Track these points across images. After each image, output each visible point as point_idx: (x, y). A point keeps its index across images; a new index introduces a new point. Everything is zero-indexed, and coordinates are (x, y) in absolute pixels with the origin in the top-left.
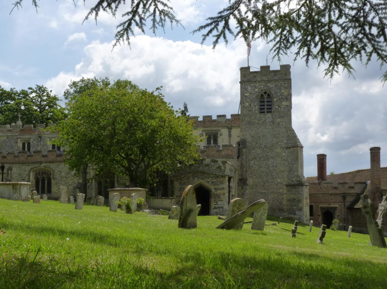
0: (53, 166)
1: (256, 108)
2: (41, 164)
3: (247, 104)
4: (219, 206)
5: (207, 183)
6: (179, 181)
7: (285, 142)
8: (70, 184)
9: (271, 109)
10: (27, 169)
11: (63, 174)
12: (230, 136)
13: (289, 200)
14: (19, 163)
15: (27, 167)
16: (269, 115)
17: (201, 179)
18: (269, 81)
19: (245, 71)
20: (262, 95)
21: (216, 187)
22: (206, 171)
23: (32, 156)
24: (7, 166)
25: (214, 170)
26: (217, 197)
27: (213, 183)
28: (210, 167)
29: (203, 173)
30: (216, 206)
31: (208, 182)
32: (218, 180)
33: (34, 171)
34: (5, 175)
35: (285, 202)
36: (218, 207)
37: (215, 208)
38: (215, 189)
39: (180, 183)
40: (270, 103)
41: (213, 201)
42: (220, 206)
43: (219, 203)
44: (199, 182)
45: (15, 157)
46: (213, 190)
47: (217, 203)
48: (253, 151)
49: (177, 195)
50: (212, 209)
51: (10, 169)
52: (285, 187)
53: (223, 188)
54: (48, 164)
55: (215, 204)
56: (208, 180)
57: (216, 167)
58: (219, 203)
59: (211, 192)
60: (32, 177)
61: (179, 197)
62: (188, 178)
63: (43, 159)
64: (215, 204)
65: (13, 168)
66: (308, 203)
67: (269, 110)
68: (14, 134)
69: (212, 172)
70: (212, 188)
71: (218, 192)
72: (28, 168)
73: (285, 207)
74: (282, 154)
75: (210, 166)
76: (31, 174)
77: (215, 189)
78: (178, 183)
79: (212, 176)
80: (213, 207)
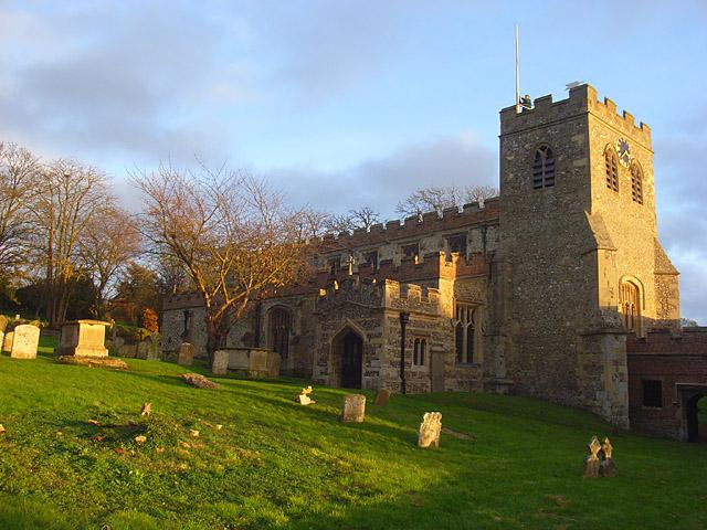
1: (527, 182)
3: (511, 176)
7: (578, 242)
9: (553, 178)
12: (485, 241)
13: (586, 367)
16: (549, 191)
18: (549, 124)
19: (507, 114)
20: (538, 155)
21: (370, 332)
29: (354, 306)
31: (359, 323)
35: (580, 372)
37: (368, 374)
39: (325, 328)
40: (552, 168)
43: (373, 363)
46: (365, 339)
47: (369, 362)
48: (521, 266)
51: (192, 315)
52: (579, 339)
53: (379, 335)
58: (373, 363)
66: (622, 374)
67: (551, 182)
73: (579, 383)
74: (573, 268)
80: (364, 371)
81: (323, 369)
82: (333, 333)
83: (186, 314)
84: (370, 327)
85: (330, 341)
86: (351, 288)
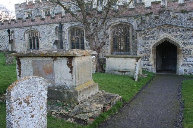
0: (39, 28)
2: (31, 27)
4: (188, 63)
5: (173, 37)
6: (143, 36)
8: (51, 41)
10: (23, 31)
11: (46, 34)
14: (18, 27)
15: (23, 29)
17: (167, 33)
21: (185, 41)
22: (174, 24)
23: (25, 21)
24: (11, 30)
25: (184, 23)
26: (187, 53)
27: (181, 37)
28: (178, 20)
29: (170, 26)
30: (186, 63)
31: (176, 36)
32: (189, 34)
33: (27, 33)
34: (10, 37)
36: (187, 64)
37: (184, 65)
38: (184, 43)
41: (182, 58)
42: (190, 63)
43: (189, 59)
44: (166, 37)
45: (16, 23)
46: (182, 46)
47: (186, 59)
49: (141, 50)
50: (180, 66)
51: (13, 32)
54: (36, 26)
55: (184, 61)
56: (176, 34)
57: (186, 19)
58: (189, 59)
59: (179, 47)
60: (27, 38)
61: (142, 53)
62: (153, 33)
63: (32, 23)
64: (184, 61)
65: (15, 31)
68: (22, 9)
69: (180, 24)
70: (180, 42)
71: (188, 47)
72: (23, 31)
75: (179, 18)
76: (26, 35)
77: (184, 43)
78: (142, 38)
79: (180, 29)
81: (145, 62)
82: (152, 43)
83: (9, 31)
84: (184, 39)
85: (151, 47)
86: (169, 15)
